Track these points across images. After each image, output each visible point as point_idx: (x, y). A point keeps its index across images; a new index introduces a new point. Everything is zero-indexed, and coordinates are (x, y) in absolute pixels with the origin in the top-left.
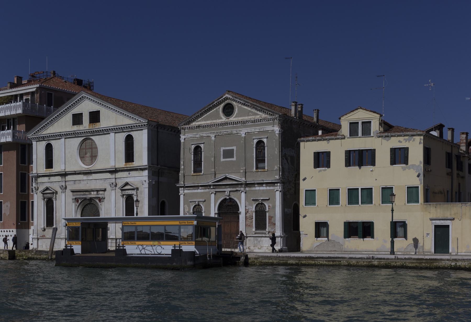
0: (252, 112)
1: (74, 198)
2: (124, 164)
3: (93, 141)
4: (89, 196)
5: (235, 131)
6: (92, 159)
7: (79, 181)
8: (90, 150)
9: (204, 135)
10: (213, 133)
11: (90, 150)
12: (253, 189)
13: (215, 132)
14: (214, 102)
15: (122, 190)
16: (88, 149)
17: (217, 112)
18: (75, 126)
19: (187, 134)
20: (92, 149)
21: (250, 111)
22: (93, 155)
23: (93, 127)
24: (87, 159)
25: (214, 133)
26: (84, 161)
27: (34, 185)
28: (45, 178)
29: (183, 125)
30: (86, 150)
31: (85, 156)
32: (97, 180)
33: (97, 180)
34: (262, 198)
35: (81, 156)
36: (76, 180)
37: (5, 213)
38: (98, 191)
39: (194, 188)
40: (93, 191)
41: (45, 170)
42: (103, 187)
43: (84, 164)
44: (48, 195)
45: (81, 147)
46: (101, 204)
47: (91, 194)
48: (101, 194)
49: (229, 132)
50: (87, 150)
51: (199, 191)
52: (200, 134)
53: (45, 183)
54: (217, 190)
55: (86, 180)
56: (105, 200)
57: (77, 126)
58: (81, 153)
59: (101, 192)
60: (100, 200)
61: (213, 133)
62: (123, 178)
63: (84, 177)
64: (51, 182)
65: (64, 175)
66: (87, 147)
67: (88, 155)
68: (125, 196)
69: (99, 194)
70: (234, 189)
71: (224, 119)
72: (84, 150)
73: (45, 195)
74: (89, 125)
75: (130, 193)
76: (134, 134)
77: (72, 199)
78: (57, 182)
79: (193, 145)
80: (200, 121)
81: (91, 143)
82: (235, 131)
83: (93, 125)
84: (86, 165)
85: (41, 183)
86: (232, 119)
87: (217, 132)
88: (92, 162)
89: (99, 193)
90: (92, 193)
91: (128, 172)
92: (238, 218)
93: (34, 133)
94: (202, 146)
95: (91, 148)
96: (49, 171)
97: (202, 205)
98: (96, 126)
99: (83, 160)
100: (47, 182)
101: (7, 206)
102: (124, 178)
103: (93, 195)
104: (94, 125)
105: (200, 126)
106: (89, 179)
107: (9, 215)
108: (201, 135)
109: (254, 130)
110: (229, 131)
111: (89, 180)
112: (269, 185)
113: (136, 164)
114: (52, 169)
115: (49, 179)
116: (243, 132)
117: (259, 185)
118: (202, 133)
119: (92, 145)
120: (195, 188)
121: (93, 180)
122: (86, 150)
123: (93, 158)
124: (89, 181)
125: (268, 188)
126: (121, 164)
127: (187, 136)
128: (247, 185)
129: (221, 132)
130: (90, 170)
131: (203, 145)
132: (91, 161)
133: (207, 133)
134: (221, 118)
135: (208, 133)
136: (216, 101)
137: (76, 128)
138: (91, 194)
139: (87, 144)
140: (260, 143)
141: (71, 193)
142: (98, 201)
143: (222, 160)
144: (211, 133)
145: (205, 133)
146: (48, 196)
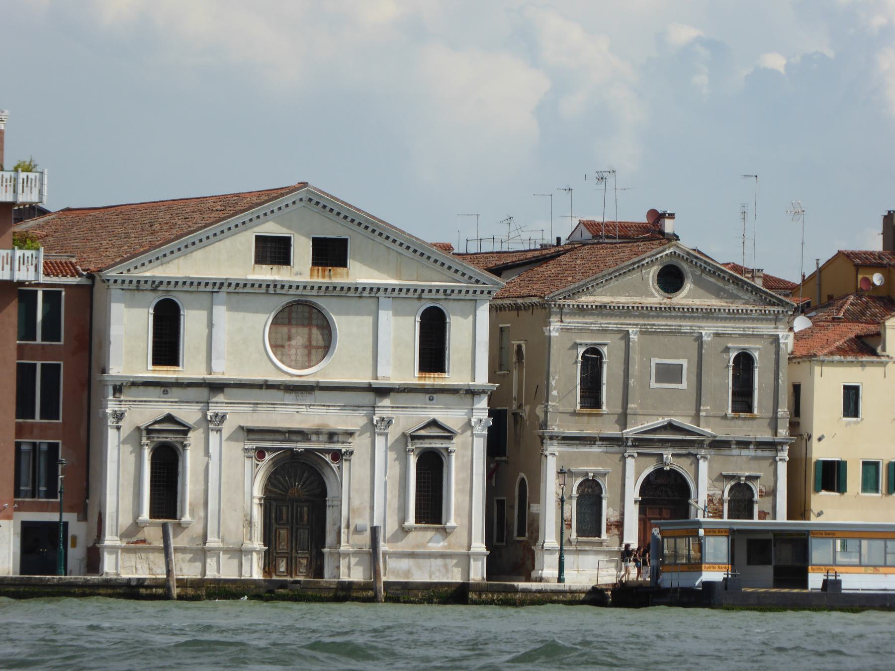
2: (417, 374)
3: (315, 311)
5: (688, 328)
6: (309, 354)
18: (264, 266)
19: (568, 320)
24: (293, 351)
25: (637, 325)
29: (560, 299)
31: (288, 343)
34: (747, 474)
35: (273, 343)
38: (332, 436)
39: (582, 442)
41: (151, 367)
46: (339, 467)
49: (673, 328)
52: (601, 324)
60: (337, 456)
65: (217, 387)
68: (417, 452)
70: (684, 452)
74: (312, 270)
82: (688, 328)
84: (290, 366)
87: (645, 325)
88: (310, 360)
91: (428, 396)
94: (605, 350)
96: (166, 373)
98: (335, 274)
104: (327, 273)
105: (605, 307)
108: (602, 325)
109: (732, 329)
111: (302, 405)
112: (761, 447)
113: (455, 376)
115: (165, 392)
117: (740, 446)
120: (586, 443)
123: (314, 351)
124: (304, 407)
126: (412, 376)
129: (654, 325)
132: (306, 359)
134: (653, 296)
135: (621, 324)
137: (267, 274)
142: (328, 458)
143: (654, 385)
144: (630, 324)
146: (166, 438)
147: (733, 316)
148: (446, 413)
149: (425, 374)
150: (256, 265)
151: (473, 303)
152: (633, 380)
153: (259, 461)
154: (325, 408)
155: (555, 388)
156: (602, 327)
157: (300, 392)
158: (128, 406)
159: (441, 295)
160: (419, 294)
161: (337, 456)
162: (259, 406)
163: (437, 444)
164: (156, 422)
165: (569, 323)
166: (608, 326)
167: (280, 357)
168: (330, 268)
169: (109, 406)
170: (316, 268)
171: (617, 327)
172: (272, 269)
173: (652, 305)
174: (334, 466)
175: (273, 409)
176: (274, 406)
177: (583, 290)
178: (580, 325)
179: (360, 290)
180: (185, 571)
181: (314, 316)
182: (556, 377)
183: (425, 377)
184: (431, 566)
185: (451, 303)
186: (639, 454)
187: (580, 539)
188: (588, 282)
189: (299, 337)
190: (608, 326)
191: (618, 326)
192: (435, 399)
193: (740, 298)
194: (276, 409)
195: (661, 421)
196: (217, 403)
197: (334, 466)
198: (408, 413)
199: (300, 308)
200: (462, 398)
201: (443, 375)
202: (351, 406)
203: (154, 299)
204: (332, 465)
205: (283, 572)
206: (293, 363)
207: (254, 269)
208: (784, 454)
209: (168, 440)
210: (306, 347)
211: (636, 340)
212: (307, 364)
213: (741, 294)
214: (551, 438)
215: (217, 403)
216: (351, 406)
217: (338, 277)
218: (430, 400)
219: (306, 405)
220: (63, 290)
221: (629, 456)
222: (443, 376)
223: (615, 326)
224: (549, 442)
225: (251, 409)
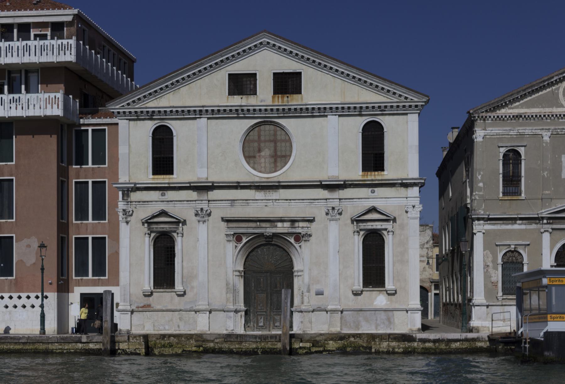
1: (232, 233)
2: (361, 173)
3: (278, 129)
4: (269, 230)
6: (275, 162)
7: (244, 202)
8: (272, 144)
9: (528, 131)
10: (546, 129)
11: (272, 144)
13: (553, 128)
14: (553, 77)
16: (265, 141)
18: (235, 97)
20: (275, 143)
22: (279, 153)
23: (283, 101)
24: (263, 160)
25: (549, 129)
26: (254, 163)
27: (121, 205)
28: (152, 193)
29: (483, 112)
30: (259, 145)
31: (258, 154)
32: (292, 201)
33: (290, 200)
35: (247, 154)
36: (236, 200)
37: (20, 262)
38: (293, 221)
39: (505, 222)
40: (282, 221)
41: (151, 176)
42: (307, 214)
43: (254, 169)
44: (162, 226)
45: (248, 137)
46: (300, 246)
47: (276, 227)
48: (301, 228)
50: (262, 145)
51: (516, 227)
52: (518, 130)
53: (151, 201)
55: (262, 200)
56: (312, 239)
57: (241, 96)
58: (247, 149)
59: (301, 224)
60: (298, 238)
61: (546, 129)
62: (359, 199)
63: (260, 195)
64: (168, 201)
66: (262, 138)
67: (266, 152)
68: (362, 233)
69: (298, 227)
72: (256, 144)
73: (154, 226)
74: (273, 98)
75: (379, 227)
76: (386, 121)
77: (226, 234)
78: (185, 202)
79: (502, 147)
80: (517, 107)
81: (272, 132)
83: (282, 98)
84: (260, 172)
85: (139, 202)
87: (556, 129)
89: (297, 224)
90: (279, 224)
91: (370, 189)
93: (128, 104)
94: (522, 150)
95: (270, 141)
96: (163, 180)
97: (521, 251)
98: (292, 100)
99: (252, 162)
100: (156, 201)
101: (29, 246)
102: (360, 200)
103: (282, 228)
104: (286, 99)
105: (521, 116)
106: (270, 198)
107: (34, 264)
108: (520, 131)
111: (270, 200)
114: (171, 176)
115: (163, 195)
118: (525, 128)
119: (275, 135)
121: (280, 201)
122: (259, 145)
123: (279, 160)
124: (271, 201)
127: (489, 132)
130: (279, 182)
131: (523, 149)
132: (273, 165)
133: (534, 128)
135: (535, 130)
136: (556, 76)
138: (276, 227)
139: (262, 133)
141: (224, 224)
142: (292, 240)
144: (543, 129)
145: (531, 128)
146: (163, 228)
148: (386, 202)
149: (368, 173)
150: (229, 96)
152: (546, 172)
153: (238, 244)
154: (288, 201)
155: (480, 181)
156: (519, 132)
157: (268, 191)
158: (135, 206)
161: (298, 238)
162: (235, 202)
163: (377, 226)
164: (154, 217)
165: (492, 130)
166: (524, 131)
167: (252, 165)
168: (288, 95)
169: (119, 206)
170: (277, 95)
171: (532, 132)
172: (242, 98)
173: (561, 113)
174: (297, 246)
175: (247, 204)
176: (247, 202)
177: (502, 104)
178: (501, 132)
180: (182, 327)
181: (279, 133)
182: (482, 173)
183: (367, 175)
184: (376, 320)
186: (553, 229)
187: (505, 297)
188: (505, 98)
189: (267, 150)
190: (524, 131)
191: (533, 131)
192: (376, 192)
194: (249, 204)
196: (202, 200)
197: (297, 246)
198: (354, 203)
199: (267, 127)
200: (398, 190)
201: (382, 173)
202: (308, 199)
204: (295, 245)
205: (262, 326)
206: (263, 169)
207: (228, 98)
209: (165, 230)
210: (272, 157)
211: (549, 141)
212: (274, 169)
214: (479, 219)
215: (202, 200)
216: (308, 199)
217: (294, 101)
218: (372, 193)
219: (272, 200)
220: (106, 128)
221: (545, 231)
222: (382, 174)
223: (531, 131)
225: (230, 204)
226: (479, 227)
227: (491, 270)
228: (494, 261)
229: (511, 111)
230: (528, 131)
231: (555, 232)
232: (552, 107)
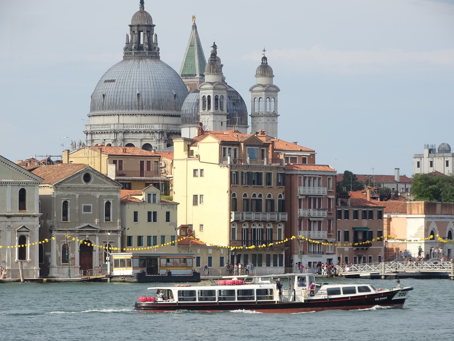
0: (103, 181)
12: (103, 234)
15: (18, 231)
17: (80, 177)
21: (102, 181)
54: (80, 234)
70: (92, 234)
71: (84, 183)
75: (25, 234)
86: (90, 184)
92: (91, 254)
94: (69, 201)
110: (89, 193)
116: (98, 195)
125: (113, 234)
128: (102, 231)
129: (83, 193)
131: (69, 200)
134: (82, 183)
140: (108, 204)
143: (83, 213)
144: (76, 193)
147: (106, 190)
151: (6, 186)
159: (25, 185)
160: (19, 184)
163: (25, 233)
179: (2, 183)
185: (28, 187)
187: (63, 264)
193: (107, 184)
195: (85, 225)
203: (19, 189)
208: (120, 234)
213: (107, 182)
214: (55, 231)
224: (54, 232)
226: (54, 233)
227: (58, 253)
228: (59, 249)
229: (65, 184)
230: (71, 193)
231: (81, 236)
232: (79, 183)
